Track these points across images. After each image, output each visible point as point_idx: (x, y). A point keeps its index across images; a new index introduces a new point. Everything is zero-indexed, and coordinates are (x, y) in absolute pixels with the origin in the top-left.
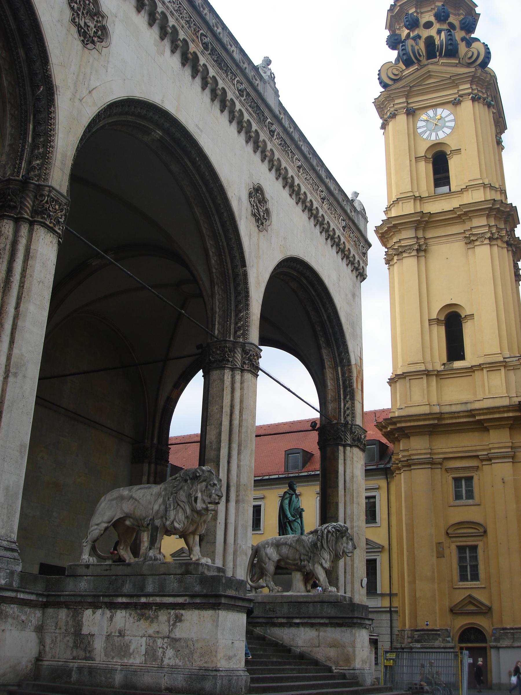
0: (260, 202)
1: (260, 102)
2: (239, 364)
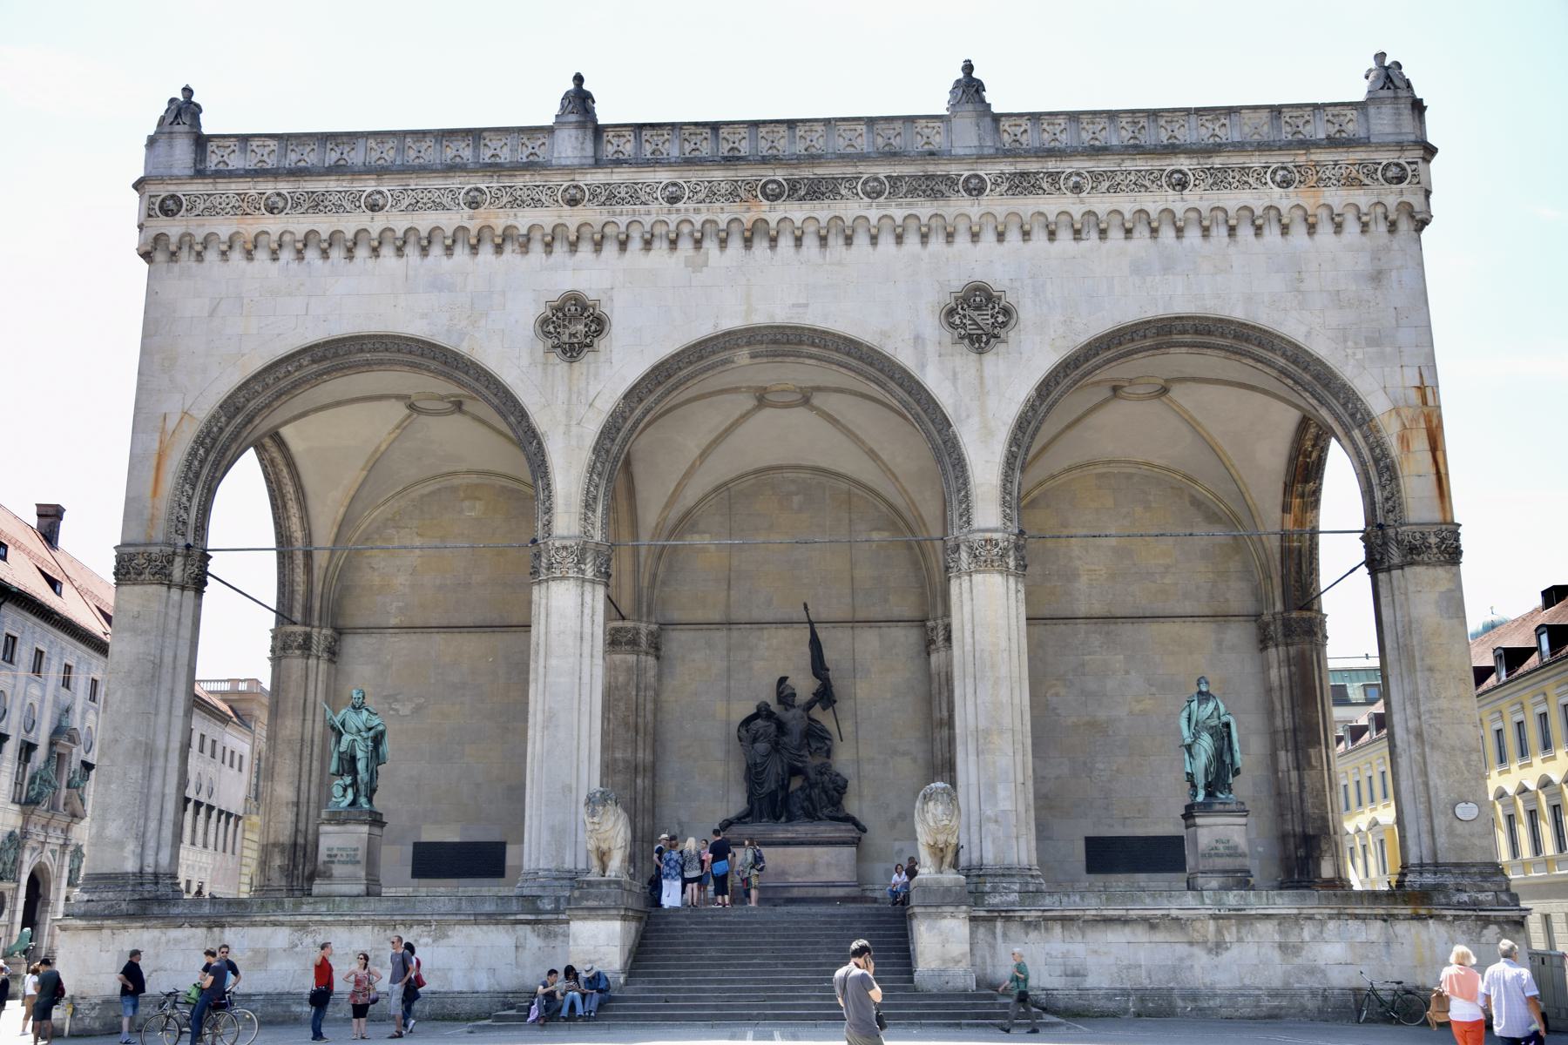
0: (978, 308)
2: (964, 566)
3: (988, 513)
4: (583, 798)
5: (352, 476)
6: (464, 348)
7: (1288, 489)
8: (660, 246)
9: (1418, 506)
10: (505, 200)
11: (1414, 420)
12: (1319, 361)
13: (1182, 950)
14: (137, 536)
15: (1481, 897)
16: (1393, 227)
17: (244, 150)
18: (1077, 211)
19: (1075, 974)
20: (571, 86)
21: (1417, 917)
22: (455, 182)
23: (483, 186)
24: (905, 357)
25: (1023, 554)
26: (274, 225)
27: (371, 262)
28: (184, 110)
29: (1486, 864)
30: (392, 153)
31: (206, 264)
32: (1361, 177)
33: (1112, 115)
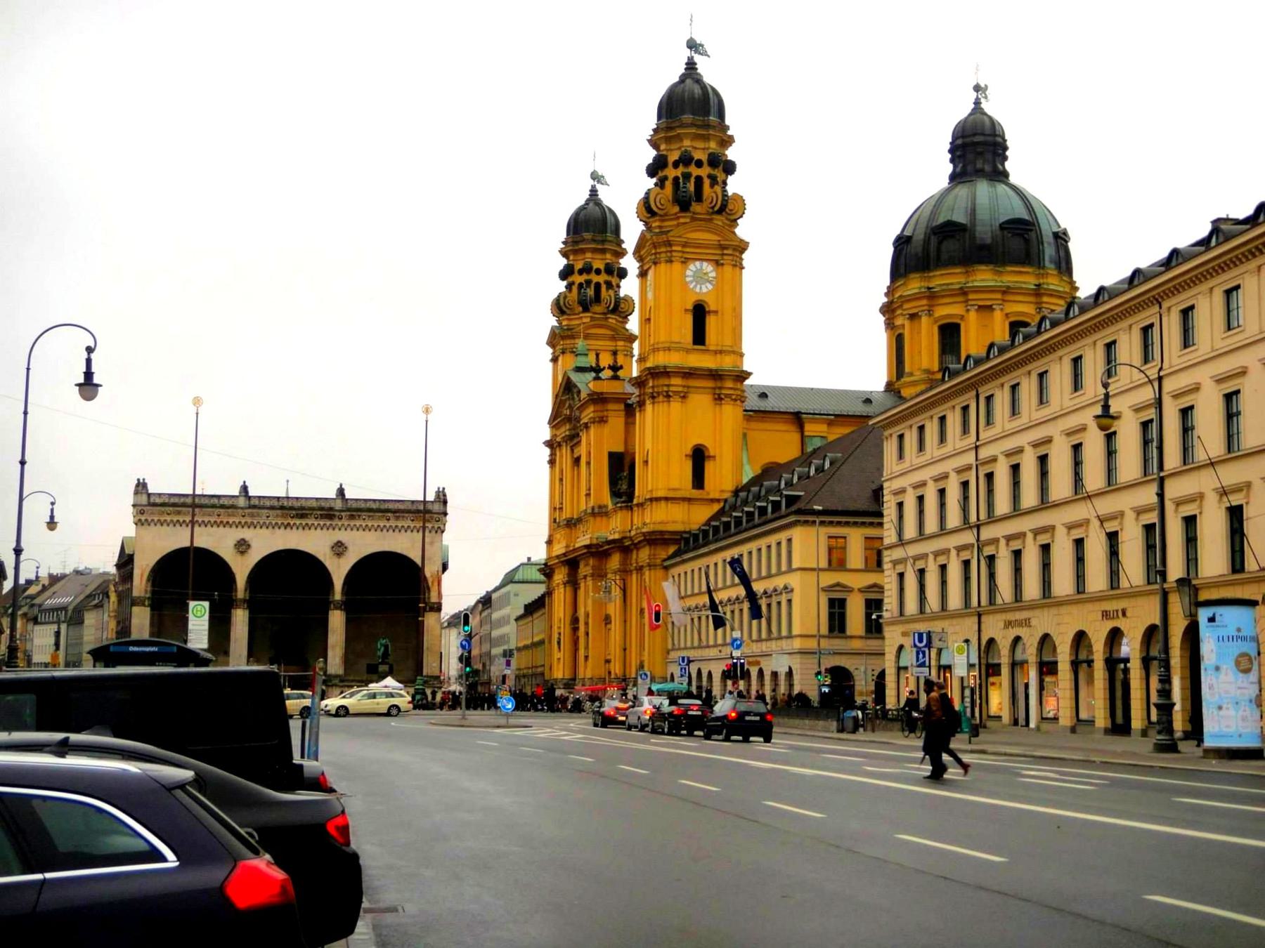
3: (338, 595)
6: (216, 551)
9: (434, 599)
24: (322, 558)
25: (347, 606)
26: (168, 518)
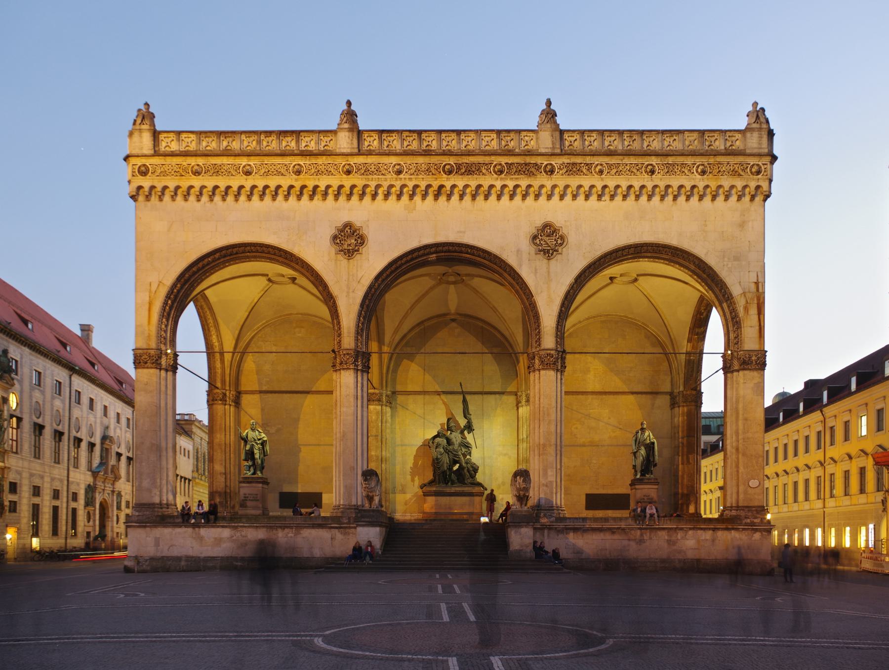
1: (529, 160)
4: (360, 473)
5: (242, 315)
7: (692, 331)
8: (393, 198)
9: (749, 344)
10: (313, 171)
11: (752, 299)
12: (710, 268)
13: (626, 543)
14: (142, 344)
15: (756, 521)
16: (753, 198)
17: (178, 140)
18: (599, 185)
19: (578, 553)
20: (345, 107)
21: (727, 529)
22: (287, 160)
23: (301, 163)
24: (512, 261)
26: (197, 182)
27: (247, 204)
28: (146, 116)
29: (759, 507)
30: (254, 143)
31: (164, 202)
32: (740, 171)
33: (621, 133)
